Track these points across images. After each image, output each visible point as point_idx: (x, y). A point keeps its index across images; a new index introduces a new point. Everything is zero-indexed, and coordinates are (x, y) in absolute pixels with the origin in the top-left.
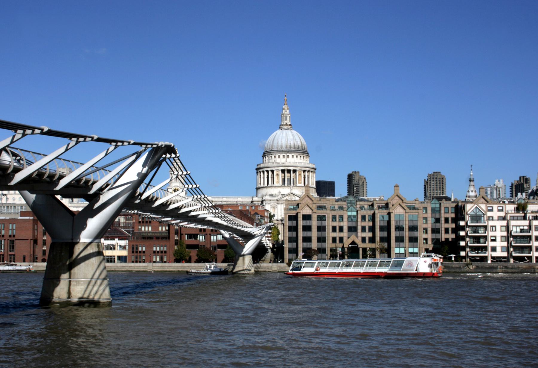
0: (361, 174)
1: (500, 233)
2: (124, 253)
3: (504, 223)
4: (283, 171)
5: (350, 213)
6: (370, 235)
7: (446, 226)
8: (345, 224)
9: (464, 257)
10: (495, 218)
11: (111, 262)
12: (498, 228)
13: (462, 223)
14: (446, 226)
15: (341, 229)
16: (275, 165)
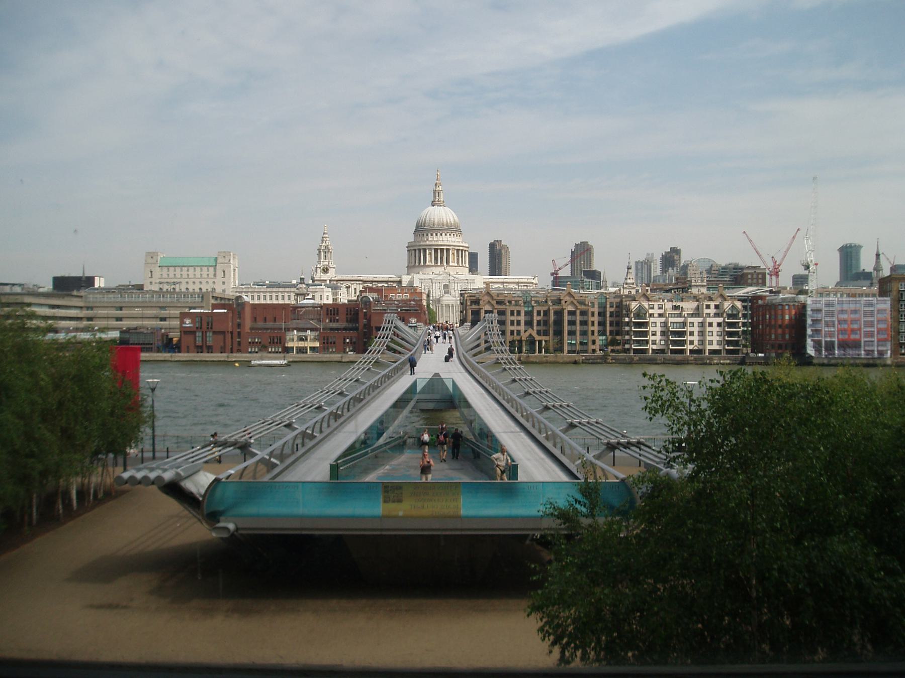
0: (503, 243)
1: (658, 329)
2: (317, 344)
3: (663, 319)
4: (436, 250)
5: (526, 309)
6: (544, 328)
8: (522, 318)
9: (628, 349)
10: (656, 315)
13: (627, 319)
14: (612, 319)
15: (519, 323)
16: (428, 243)
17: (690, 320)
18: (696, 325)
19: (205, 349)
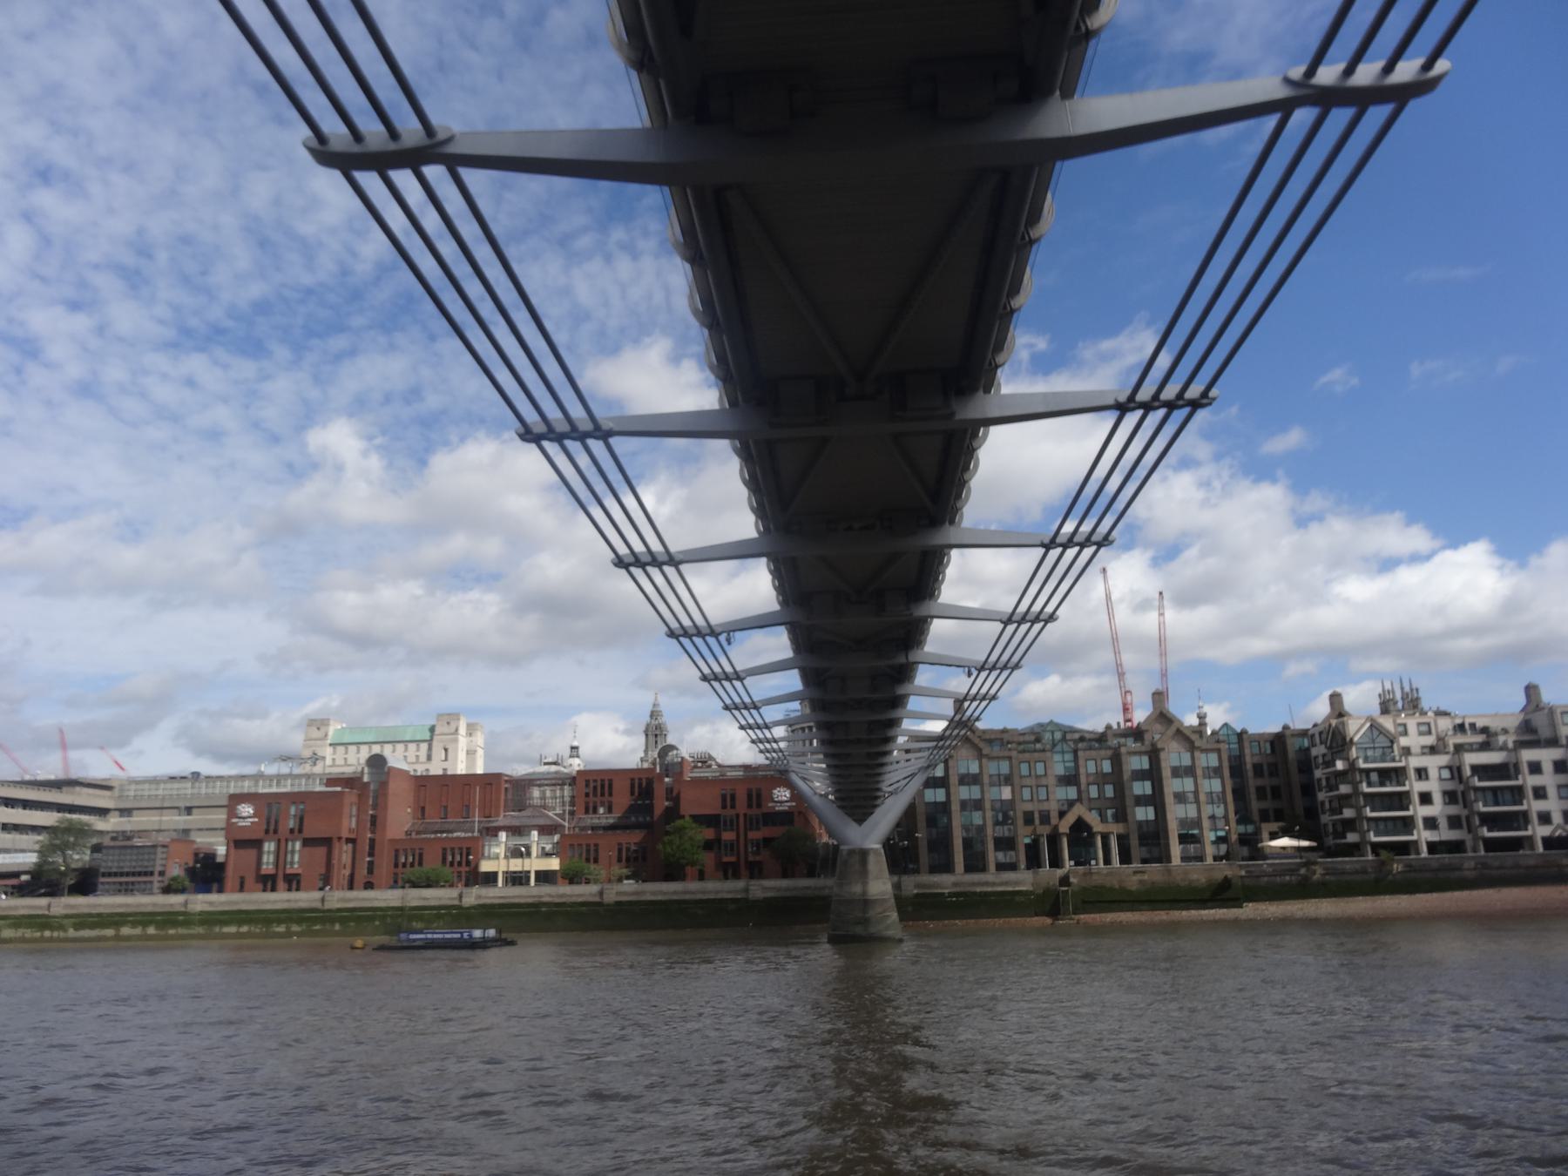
2: (554, 864)
3: (1443, 760)
7: (1260, 782)
9: (1354, 849)
11: (521, 884)
12: (1433, 773)
17: (1528, 755)
18: (1548, 767)
19: (281, 884)
